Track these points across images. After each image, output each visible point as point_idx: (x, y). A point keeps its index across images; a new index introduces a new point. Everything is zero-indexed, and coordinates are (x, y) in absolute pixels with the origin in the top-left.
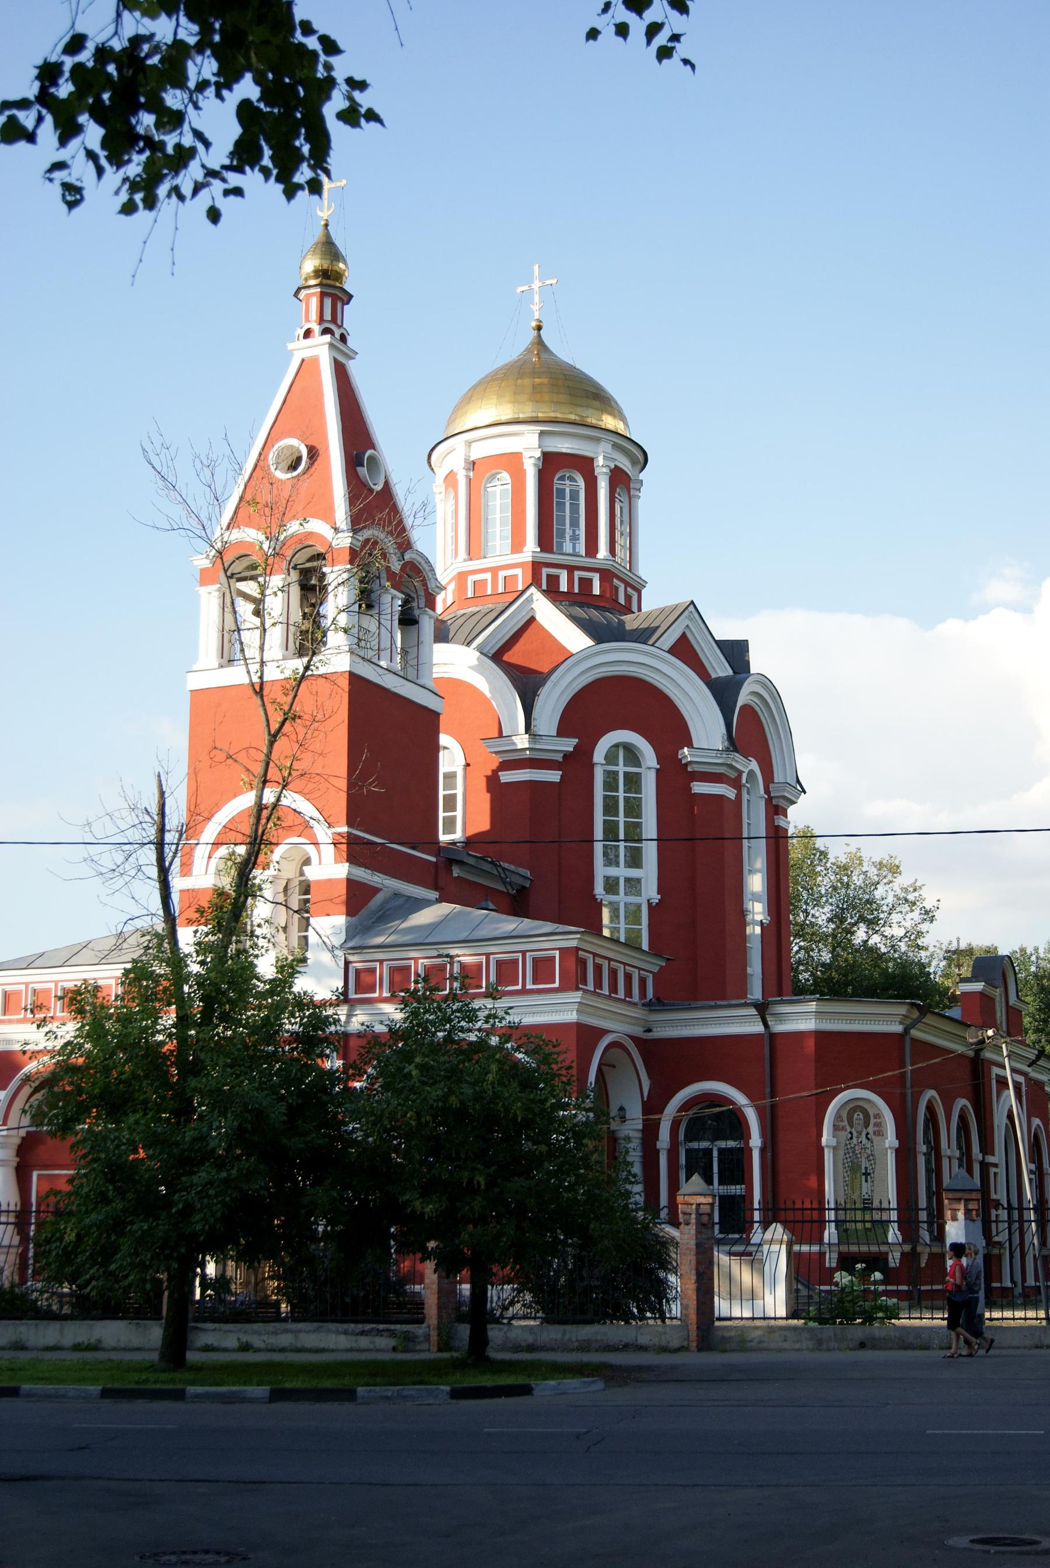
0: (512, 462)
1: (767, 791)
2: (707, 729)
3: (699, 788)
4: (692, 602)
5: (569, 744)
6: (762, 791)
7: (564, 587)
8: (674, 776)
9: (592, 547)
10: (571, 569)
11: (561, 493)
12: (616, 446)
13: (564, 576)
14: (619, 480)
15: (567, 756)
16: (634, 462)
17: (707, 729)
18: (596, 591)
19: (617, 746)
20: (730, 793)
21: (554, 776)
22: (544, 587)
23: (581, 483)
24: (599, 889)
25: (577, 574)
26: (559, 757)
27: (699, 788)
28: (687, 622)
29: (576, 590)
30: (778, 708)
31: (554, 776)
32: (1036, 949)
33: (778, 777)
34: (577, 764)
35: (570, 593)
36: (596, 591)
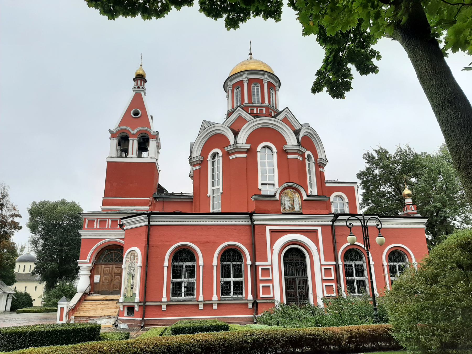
0: (241, 82)
1: (316, 160)
2: (291, 140)
4: (287, 108)
5: (248, 146)
6: (313, 161)
7: (255, 112)
8: (283, 153)
10: (257, 107)
12: (269, 76)
13: (255, 109)
14: (269, 84)
15: (248, 150)
16: (276, 82)
17: (291, 140)
18: (264, 112)
19: (264, 147)
20: (301, 159)
21: (244, 156)
22: (249, 112)
25: (259, 109)
26: (246, 150)
28: (286, 113)
29: (259, 113)
30: (317, 136)
32: (297, 14)
33: (320, 157)
34: (251, 152)
36: (264, 112)
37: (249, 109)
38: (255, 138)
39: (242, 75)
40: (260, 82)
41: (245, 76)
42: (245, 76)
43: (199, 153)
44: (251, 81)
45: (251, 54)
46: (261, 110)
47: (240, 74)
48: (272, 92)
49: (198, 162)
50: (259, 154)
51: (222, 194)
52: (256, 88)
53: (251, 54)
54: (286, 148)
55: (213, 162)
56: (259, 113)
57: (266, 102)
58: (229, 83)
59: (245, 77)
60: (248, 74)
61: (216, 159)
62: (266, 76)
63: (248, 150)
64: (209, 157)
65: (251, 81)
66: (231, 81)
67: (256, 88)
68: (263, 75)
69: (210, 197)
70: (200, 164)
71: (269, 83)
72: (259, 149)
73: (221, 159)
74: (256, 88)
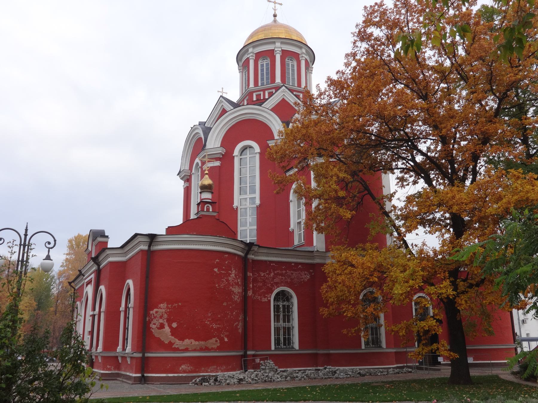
0: (271, 54)
9: (299, 85)
12: (306, 51)
39: (274, 43)
40: (296, 56)
41: (278, 44)
42: (278, 44)
44: (285, 54)
45: (275, 16)
47: (272, 40)
51: (260, 205)
52: (291, 64)
53: (275, 16)
55: (241, 159)
57: (303, 85)
58: (250, 50)
59: (278, 47)
60: (282, 43)
61: (248, 155)
62: (304, 51)
64: (236, 152)
65: (285, 54)
66: (254, 47)
68: (301, 48)
69: (237, 208)
71: (306, 61)
73: (258, 156)
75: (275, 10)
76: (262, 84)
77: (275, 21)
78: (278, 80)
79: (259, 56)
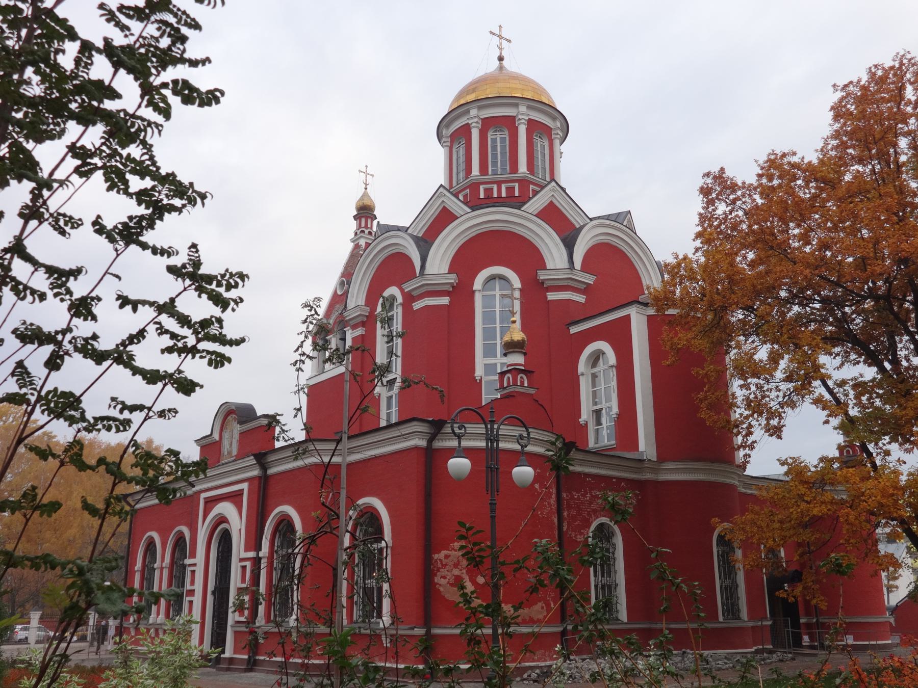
3: (552, 296)
5: (452, 279)
7: (495, 195)
8: (534, 290)
9: (514, 167)
10: (499, 183)
11: (494, 141)
12: (529, 107)
13: (495, 187)
14: (533, 126)
16: (554, 119)
18: (517, 194)
19: (492, 278)
21: (445, 301)
23: (507, 132)
24: (479, 372)
27: (552, 296)
31: (445, 301)
34: (461, 294)
35: (499, 196)
36: (517, 194)
37: (482, 188)
38: (467, 260)
39: (468, 112)
40: (510, 123)
42: (474, 112)
43: (362, 301)
44: (488, 124)
45: (501, 59)
46: (510, 190)
48: (541, 144)
49: (359, 320)
50: (478, 298)
52: (498, 137)
53: (501, 59)
54: (542, 275)
56: (504, 194)
57: (523, 168)
59: (474, 117)
60: (480, 108)
62: (523, 109)
63: (453, 287)
66: (448, 126)
67: (498, 137)
68: (517, 105)
70: (363, 324)
72: (478, 284)
74: (498, 137)
75: (501, 49)
76: (495, 173)
77: (501, 68)
78: (476, 171)
79: (454, 137)
